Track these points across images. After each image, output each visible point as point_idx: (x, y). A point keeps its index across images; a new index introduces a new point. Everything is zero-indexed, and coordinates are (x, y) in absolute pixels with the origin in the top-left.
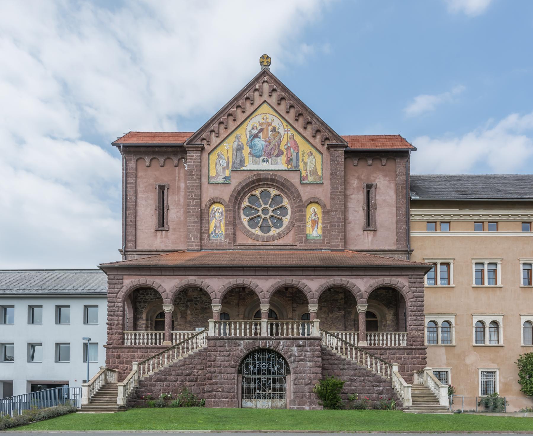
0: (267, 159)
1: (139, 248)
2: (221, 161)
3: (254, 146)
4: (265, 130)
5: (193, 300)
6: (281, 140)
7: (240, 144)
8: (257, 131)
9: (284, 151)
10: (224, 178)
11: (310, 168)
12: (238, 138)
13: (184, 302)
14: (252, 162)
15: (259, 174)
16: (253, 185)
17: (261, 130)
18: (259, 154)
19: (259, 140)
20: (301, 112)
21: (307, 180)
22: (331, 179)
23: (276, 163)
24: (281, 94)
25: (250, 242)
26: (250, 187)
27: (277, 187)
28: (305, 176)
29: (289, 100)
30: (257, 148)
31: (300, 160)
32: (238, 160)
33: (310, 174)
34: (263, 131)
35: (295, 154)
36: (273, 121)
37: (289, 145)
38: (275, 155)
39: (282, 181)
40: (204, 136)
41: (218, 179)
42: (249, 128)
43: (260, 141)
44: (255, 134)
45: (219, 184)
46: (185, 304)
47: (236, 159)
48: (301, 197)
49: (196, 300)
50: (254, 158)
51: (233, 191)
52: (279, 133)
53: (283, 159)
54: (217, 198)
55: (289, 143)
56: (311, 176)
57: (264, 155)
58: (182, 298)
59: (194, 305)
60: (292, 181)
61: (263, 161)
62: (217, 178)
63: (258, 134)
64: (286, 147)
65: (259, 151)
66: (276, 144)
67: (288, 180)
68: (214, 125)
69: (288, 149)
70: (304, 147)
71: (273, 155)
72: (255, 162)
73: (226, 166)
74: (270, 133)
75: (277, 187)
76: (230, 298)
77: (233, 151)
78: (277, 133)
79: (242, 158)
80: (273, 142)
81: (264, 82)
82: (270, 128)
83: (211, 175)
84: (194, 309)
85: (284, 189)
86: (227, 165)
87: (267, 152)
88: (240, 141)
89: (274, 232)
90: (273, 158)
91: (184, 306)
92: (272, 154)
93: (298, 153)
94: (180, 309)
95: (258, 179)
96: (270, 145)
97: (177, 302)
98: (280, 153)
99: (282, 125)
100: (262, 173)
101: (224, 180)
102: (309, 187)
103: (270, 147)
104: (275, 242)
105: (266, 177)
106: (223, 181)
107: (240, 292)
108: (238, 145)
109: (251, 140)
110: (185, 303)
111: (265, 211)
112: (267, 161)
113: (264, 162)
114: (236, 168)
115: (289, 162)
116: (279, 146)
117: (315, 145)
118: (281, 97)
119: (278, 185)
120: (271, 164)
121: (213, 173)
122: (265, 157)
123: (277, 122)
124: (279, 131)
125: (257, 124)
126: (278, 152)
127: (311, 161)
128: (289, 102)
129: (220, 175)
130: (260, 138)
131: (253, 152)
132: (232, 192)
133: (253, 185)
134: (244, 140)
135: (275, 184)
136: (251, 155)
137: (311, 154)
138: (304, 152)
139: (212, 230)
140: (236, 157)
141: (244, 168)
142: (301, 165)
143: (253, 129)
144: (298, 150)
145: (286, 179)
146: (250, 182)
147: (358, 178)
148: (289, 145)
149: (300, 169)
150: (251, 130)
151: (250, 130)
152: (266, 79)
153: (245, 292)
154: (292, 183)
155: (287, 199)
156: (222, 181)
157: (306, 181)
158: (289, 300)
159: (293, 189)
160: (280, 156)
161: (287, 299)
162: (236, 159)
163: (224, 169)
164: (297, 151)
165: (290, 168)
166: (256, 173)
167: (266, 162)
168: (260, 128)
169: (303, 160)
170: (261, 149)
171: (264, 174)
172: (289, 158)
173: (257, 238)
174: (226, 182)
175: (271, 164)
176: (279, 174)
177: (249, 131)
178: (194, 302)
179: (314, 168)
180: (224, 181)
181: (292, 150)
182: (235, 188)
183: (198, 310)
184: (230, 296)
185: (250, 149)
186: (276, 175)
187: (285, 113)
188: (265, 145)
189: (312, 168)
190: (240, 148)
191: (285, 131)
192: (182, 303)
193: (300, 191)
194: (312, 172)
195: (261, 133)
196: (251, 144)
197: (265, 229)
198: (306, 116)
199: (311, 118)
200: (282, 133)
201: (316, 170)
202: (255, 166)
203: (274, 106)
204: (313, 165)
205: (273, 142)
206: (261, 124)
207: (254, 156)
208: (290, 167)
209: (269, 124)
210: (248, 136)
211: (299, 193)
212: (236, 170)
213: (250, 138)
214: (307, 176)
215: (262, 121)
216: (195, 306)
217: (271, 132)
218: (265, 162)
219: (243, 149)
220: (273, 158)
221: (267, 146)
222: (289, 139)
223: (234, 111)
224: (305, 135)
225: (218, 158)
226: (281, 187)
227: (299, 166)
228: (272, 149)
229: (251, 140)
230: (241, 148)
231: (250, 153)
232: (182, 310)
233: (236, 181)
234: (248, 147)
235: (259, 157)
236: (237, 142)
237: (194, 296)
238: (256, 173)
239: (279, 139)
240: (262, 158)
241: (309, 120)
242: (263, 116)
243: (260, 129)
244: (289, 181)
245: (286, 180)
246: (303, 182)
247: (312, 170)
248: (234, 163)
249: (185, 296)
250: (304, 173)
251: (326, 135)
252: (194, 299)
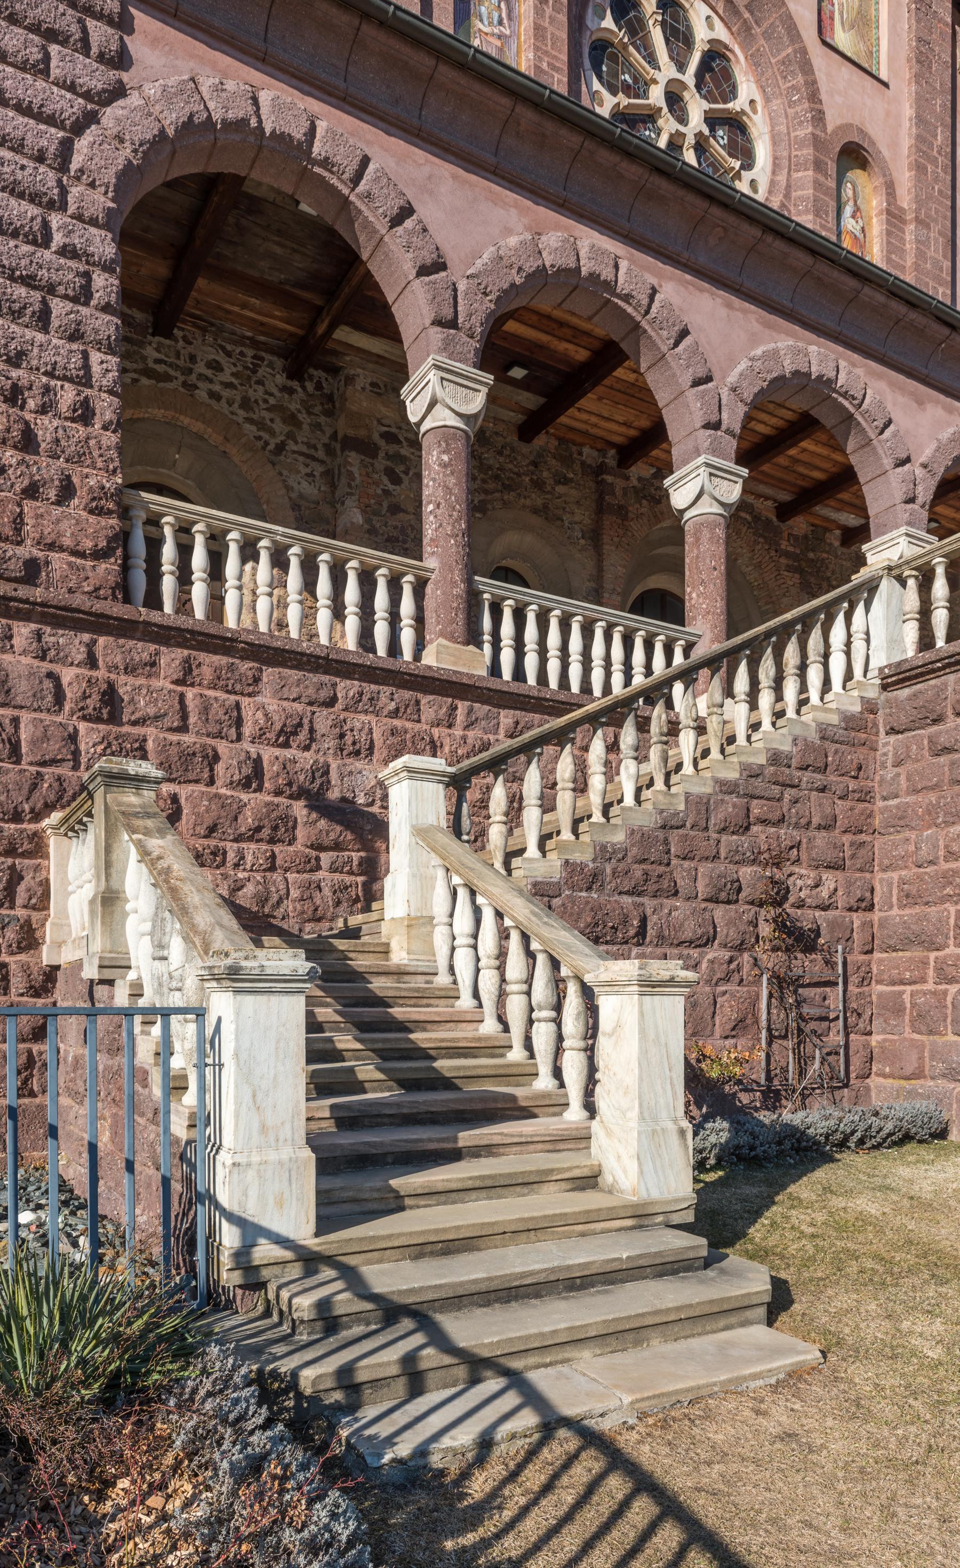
5: (377, 448)
13: (315, 447)
46: (322, 462)
49: (392, 449)
58: (302, 417)
59: (385, 480)
76: (560, 489)
84: (385, 504)
91: (310, 475)
94: (291, 482)
97: (273, 433)
107: (601, 469)
110: (321, 454)
153: (627, 478)
158: (789, 568)
161: (783, 561)
178: (381, 463)
183: (401, 515)
184: (559, 482)
192: (304, 449)
216: (391, 487)
232: (301, 496)
237: (380, 422)
249: (317, 409)
252: (382, 443)
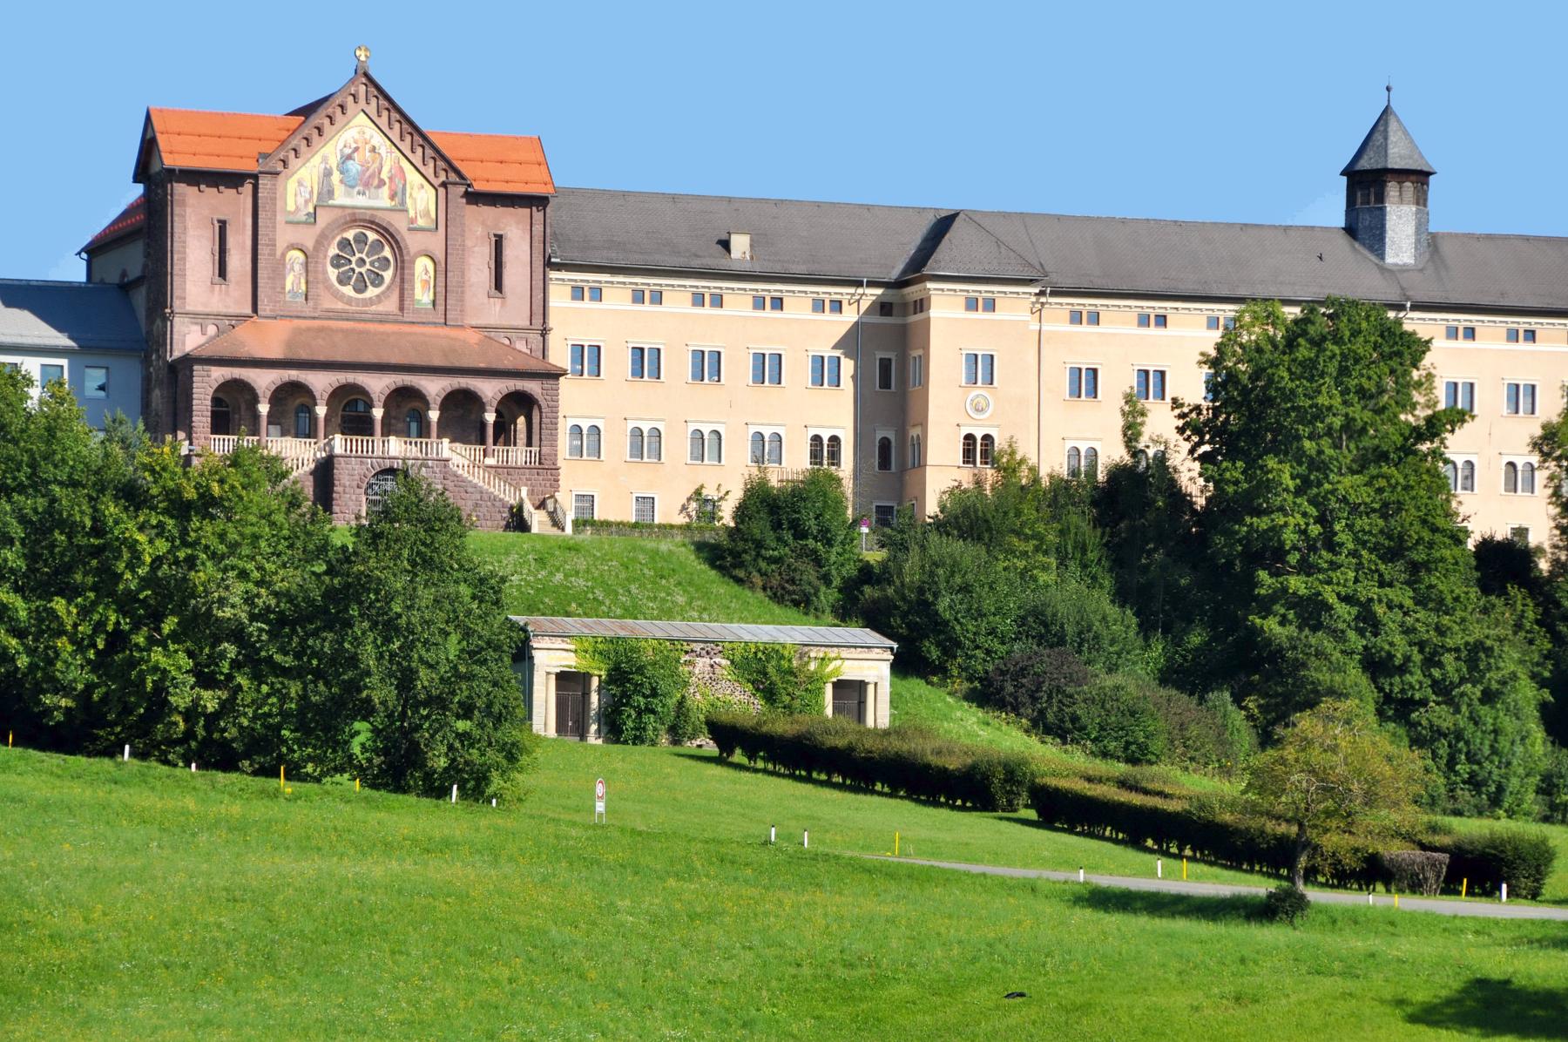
1: (189, 308)
9: (387, 181)
11: (421, 206)
12: (325, 159)
15: (354, 214)
17: (356, 149)
18: (352, 183)
23: (377, 197)
25: (340, 306)
36: (372, 137)
42: (341, 145)
53: (385, 191)
61: (359, 193)
69: (391, 178)
70: (413, 177)
72: (349, 195)
74: (368, 154)
82: (368, 147)
89: (372, 292)
90: (372, 190)
93: (404, 185)
98: (382, 183)
103: (368, 174)
104: (374, 308)
111: (362, 262)
112: (364, 194)
115: (392, 197)
121: (291, 207)
123: (378, 139)
125: (351, 141)
134: (333, 162)
137: (422, 187)
139: (288, 286)
141: (331, 202)
142: (408, 201)
147: (483, 223)
163: (306, 202)
166: (350, 211)
168: (354, 146)
173: (349, 301)
176: (379, 214)
190: (328, 174)
197: (361, 287)
200: (384, 155)
215: (357, 136)
220: (372, 190)
221: (364, 172)
231: (342, 181)
233: (324, 218)
235: (352, 187)
242: (358, 129)
248: (319, 194)
250: (412, 213)
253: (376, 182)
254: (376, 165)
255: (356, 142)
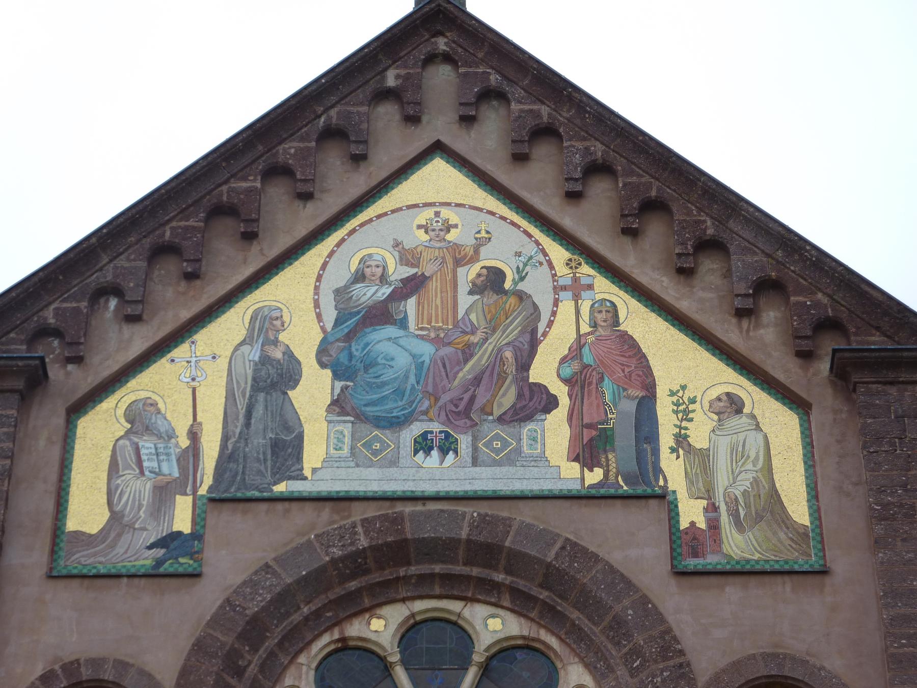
0: (448, 435)
2: (147, 445)
3: (366, 368)
4: (434, 285)
6: (534, 331)
7: (278, 354)
8: (386, 291)
9: (560, 390)
10: (162, 543)
14: (346, 451)
15: (397, 520)
16: (353, 585)
18: (394, 407)
19: (401, 333)
20: (653, 193)
21: (713, 552)
22: (878, 543)
24: (531, 111)
26: (332, 596)
27: (515, 592)
28: (702, 525)
29: (584, 139)
30: (384, 378)
31: (666, 440)
32: (259, 442)
33: (734, 515)
34: (422, 292)
35: (630, 407)
37: (588, 358)
38: (497, 412)
39: (550, 557)
40: (50, 316)
41: (120, 549)
42: (338, 276)
43: (402, 342)
44: (370, 302)
45: (118, 576)
47: (244, 437)
48: (682, 653)
50: (364, 428)
51: (216, 621)
52: (521, 296)
54: (96, 663)
55: (585, 350)
56: (738, 524)
57: (426, 413)
60: (616, 557)
61: (423, 444)
62: (113, 546)
63: (392, 307)
64: (567, 372)
65: (399, 393)
66: (508, 354)
67: (585, 551)
68: (122, 262)
71: (486, 410)
73: (176, 474)
74: (465, 301)
75: (515, 592)
77: (230, 396)
78: (512, 300)
79: (288, 428)
80: (489, 347)
81: (431, 59)
82: (469, 274)
83: (72, 524)
85: (562, 606)
86: (183, 469)
87: (445, 398)
88: (276, 342)
90: (491, 430)
92: (478, 404)
95: (387, 545)
96: (466, 361)
99: (541, 257)
100: (413, 514)
101: (160, 552)
102: (733, 591)
103: (467, 371)
105: (443, 532)
106: (149, 562)
108: (265, 360)
109: (349, 337)
112: (447, 446)
113: (428, 451)
114: (244, 485)
116: (524, 366)
117: (757, 357)
118: (531, 123)
119: (522, 584)
120: (475, 462)
122: (436, 427)
124: (521, 286)
126: (520, 396)
127: (733, 449)
128: (579, 145)
129: (131, 526)
130: (403, 324)
131: (360, 398)
132: (208, 624)
133: (353, 585)
135: (500, 577)
136: (343, 412)
138: (688, 394)
140: (248, 424)
143: (360, 277)
144: (650, 388)
145: (575, 544)
146: (334, 561)
148: (588, 358)
149: (665, 487)
150: (346, 287)
151: (342, 284)
152: (442, 44)
154: (613, 570)
155: (587, 666)
156: (146, 560)
157: (711, 560)
159: (626, 602)
160: (529, 418)
162: (244, 437)
164: (641, 394)
165: (600, 485)
166: (371, 510)
167: (444, 452)
169: (681, 440)
170: (412, 379)
171: (429, 515)
172: (590, 426)
174: (167, 567)
175: (475, 462)
176: (525, 514)
177: (338, 292)
179: (756, 481)
180: (159, 563)
181: (608, 387)
182: (228, 601)
185: (339, 385)
186: (507, 523)
187: (557, 201)
188: (433, 360)
189: (745, 483)
191: (557, 289)
193: (671, 619)
194: (748, 506)
195: (411, 303)
196: (343, 358)
198: (690, 213)
199: (720, 222)
200: (544, 303)
201: (774, 495)
202: (373, 473)
203: (489, 168)
204: (749, 466)
205: (489, 347)
206: (407, 257)
207: (360, 417)
208: (595, 476)
209: (461, 258)
210: (330, 316)
211: (669, 631)
212: (239, 495)
213: (338, 323)
214: (714, 525)
217: (471, 293)
218: (435, 453)
219: (297, 382)
220: (491, 430)
221: (447, 368)
222: (585, 328)
223: (249, 191)
224: (685, 305)
225: (128, 432)
226: (544, 595)
227: (658, 471)
228: (477, 381)
229: (349, 337)
230: (281, 375)
231: (338, 406)
234: (328, 373)
235: (396, 423)
236: (258, 346)
238: (371, 510)
239: (522, 332)
240: (416, 429)
241: (710, 232)
243: (406, 281)
244: (596, 558)
245: (575, 550)
246: (692, 563)
247: (745, 493)
248: (226, 458)
251: (817, 305)
253: (507, 398)
254: (513, 330)
255: (407, 257)
